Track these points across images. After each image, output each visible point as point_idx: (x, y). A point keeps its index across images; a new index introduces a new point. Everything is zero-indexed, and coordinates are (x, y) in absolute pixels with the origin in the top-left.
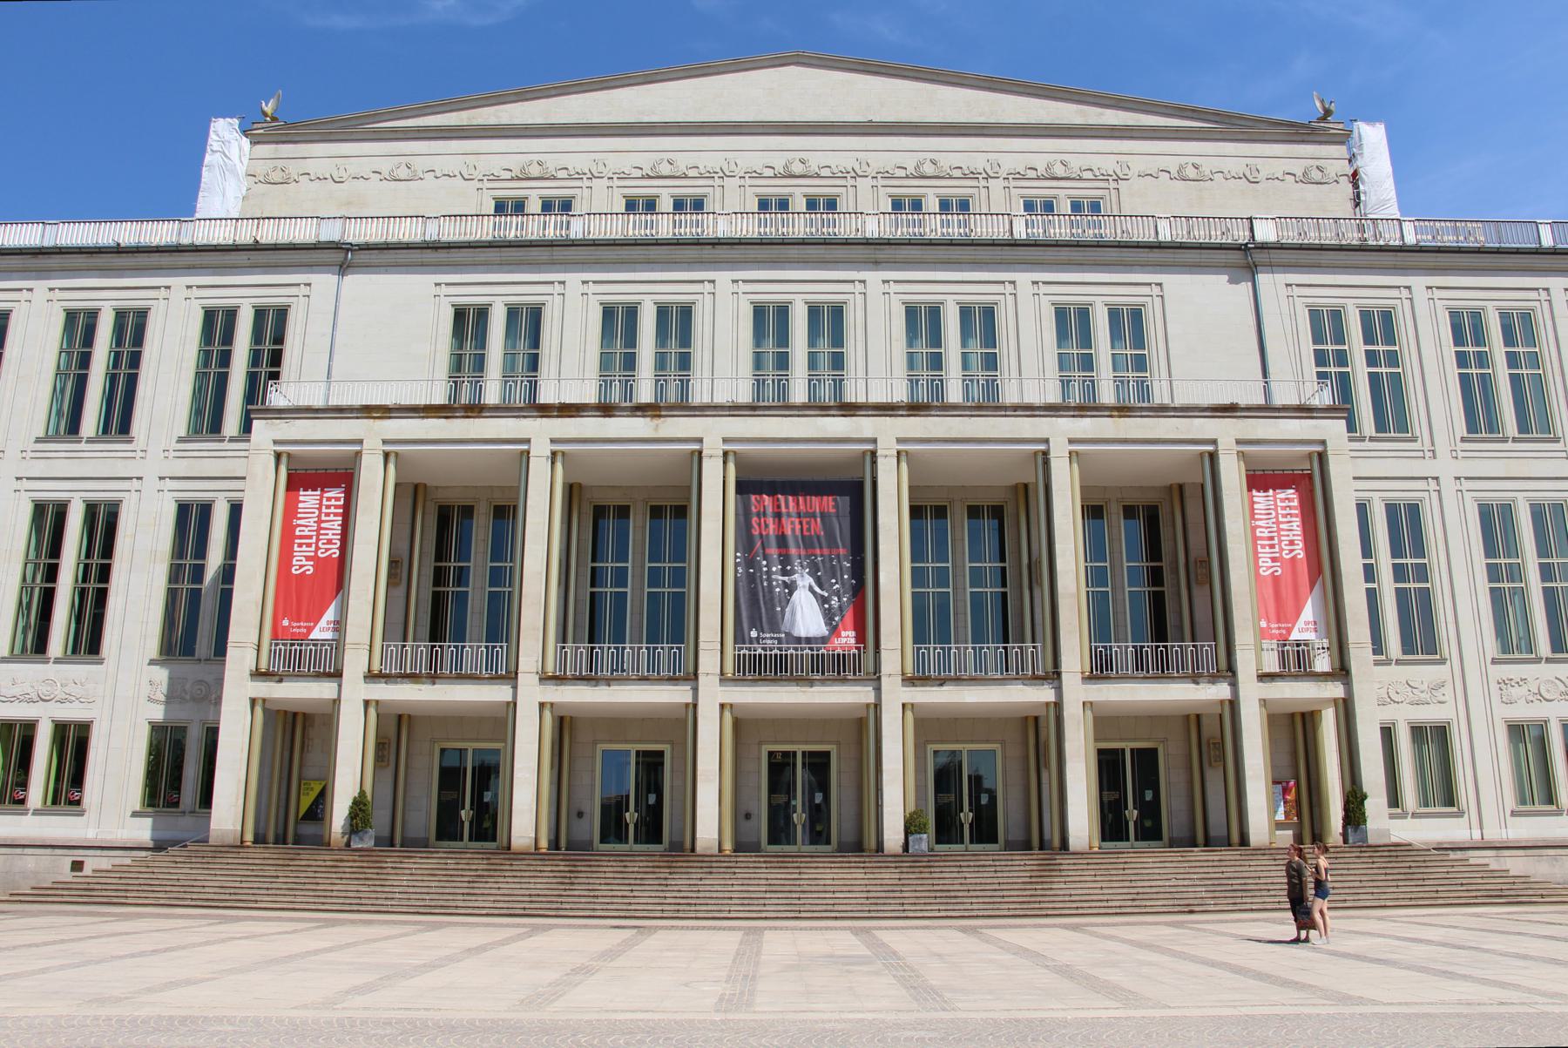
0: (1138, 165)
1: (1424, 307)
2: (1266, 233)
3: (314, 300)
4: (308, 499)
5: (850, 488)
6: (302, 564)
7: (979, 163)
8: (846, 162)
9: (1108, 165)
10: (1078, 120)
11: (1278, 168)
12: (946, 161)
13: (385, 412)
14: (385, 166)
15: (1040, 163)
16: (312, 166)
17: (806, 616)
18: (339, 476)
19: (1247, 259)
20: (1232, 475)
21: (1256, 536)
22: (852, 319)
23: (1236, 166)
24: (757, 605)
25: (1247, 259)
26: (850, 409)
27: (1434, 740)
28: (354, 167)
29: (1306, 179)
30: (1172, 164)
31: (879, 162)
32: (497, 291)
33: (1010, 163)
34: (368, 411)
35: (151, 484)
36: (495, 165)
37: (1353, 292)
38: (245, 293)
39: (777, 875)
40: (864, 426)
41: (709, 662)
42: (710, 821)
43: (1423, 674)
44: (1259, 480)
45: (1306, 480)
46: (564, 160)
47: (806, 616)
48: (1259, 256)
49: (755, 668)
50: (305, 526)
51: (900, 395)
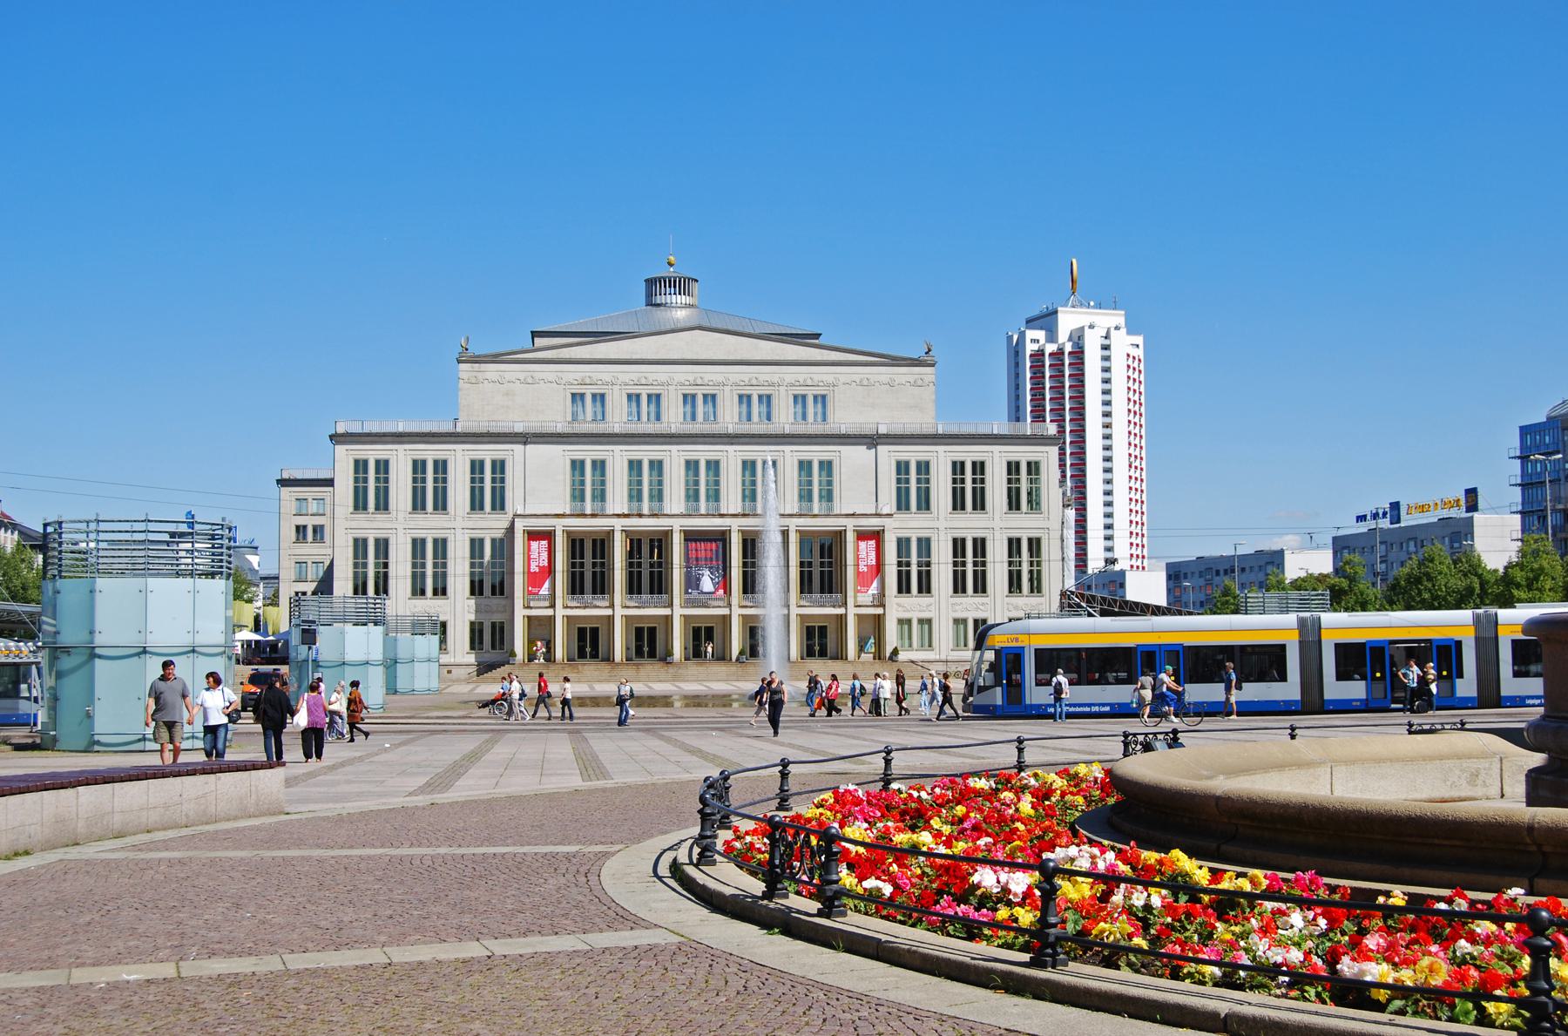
0: (843, 379)
1: (941, 459)
2: (883, 430)
3: (514, 454)
4: (534, 545)
5: (722, 538)
6: (534, 568)
7: (775, 379)
8: (720, 378)
9: (830, 379)
11: (903, 379)
12: (762, 378)
13: (563, 516)
14: (522, 376)
16: (488, 375)
17: (707, 584)
18: (548, 536)
19: (872, 440)
20: (850, 537)
21: (859, 555)
22: (723, 466)
23: (885, 379)
24: (692, 582)
25: (872, 440)
26: (722, 516)
27: (926, 622)
28: (508, 376)
29: (915, 385)
30: (857, 378)
31: (734, 378)
32: (589, 453)
33: (789, 379)
34: (557, 516)
35: (459, 532)
36: (570, 377)
37: (913, 454)
38: (488, 453)
39: (701, 669)
40: (727, 522)
41: (676, 601)
42: (619, 653)
43: (924, 600)
44: (862, 536)
45: (877, 536)
46: (600, 376)
47: (707, 584)
49: (689, 603)
50: (534, 555)
51: (739, 510)
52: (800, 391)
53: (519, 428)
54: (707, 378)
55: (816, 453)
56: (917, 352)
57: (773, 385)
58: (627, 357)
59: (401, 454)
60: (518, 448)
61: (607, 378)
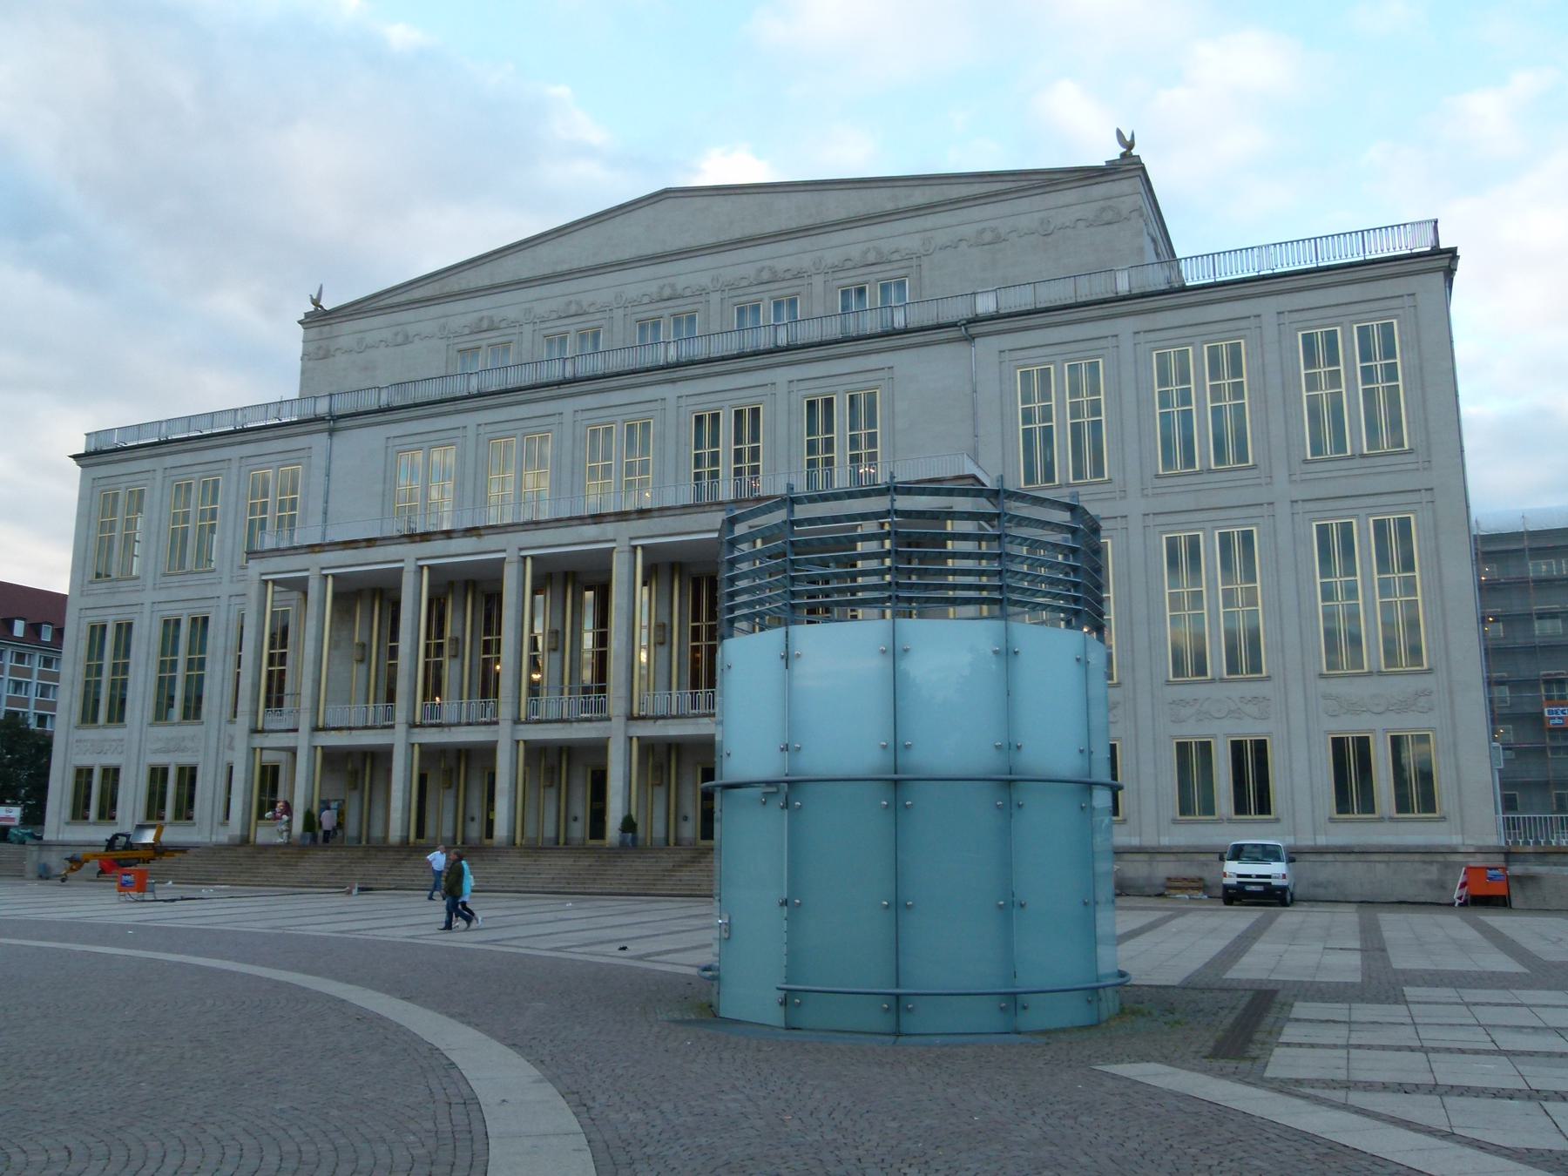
7: (806, 262)
8: (704, 280)
9: (913, 243)
10: (889, 206)
12: (781, 265)
15: (855, 252)
19: (968, 329)
25: (968, 329)
33: (832, 258)
40: (609, 529)
48: (972, 331)
52: (851, 279)
53: (322, 407)
54: (681, 283)
55: (837, 378)
56: (1105, 152)
57: (798, 276)
58: (547, 271)
59: (159, 475)
60: (318, 441)
61: (512, 313)
